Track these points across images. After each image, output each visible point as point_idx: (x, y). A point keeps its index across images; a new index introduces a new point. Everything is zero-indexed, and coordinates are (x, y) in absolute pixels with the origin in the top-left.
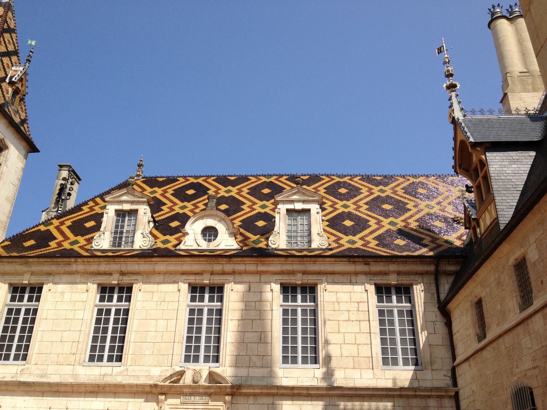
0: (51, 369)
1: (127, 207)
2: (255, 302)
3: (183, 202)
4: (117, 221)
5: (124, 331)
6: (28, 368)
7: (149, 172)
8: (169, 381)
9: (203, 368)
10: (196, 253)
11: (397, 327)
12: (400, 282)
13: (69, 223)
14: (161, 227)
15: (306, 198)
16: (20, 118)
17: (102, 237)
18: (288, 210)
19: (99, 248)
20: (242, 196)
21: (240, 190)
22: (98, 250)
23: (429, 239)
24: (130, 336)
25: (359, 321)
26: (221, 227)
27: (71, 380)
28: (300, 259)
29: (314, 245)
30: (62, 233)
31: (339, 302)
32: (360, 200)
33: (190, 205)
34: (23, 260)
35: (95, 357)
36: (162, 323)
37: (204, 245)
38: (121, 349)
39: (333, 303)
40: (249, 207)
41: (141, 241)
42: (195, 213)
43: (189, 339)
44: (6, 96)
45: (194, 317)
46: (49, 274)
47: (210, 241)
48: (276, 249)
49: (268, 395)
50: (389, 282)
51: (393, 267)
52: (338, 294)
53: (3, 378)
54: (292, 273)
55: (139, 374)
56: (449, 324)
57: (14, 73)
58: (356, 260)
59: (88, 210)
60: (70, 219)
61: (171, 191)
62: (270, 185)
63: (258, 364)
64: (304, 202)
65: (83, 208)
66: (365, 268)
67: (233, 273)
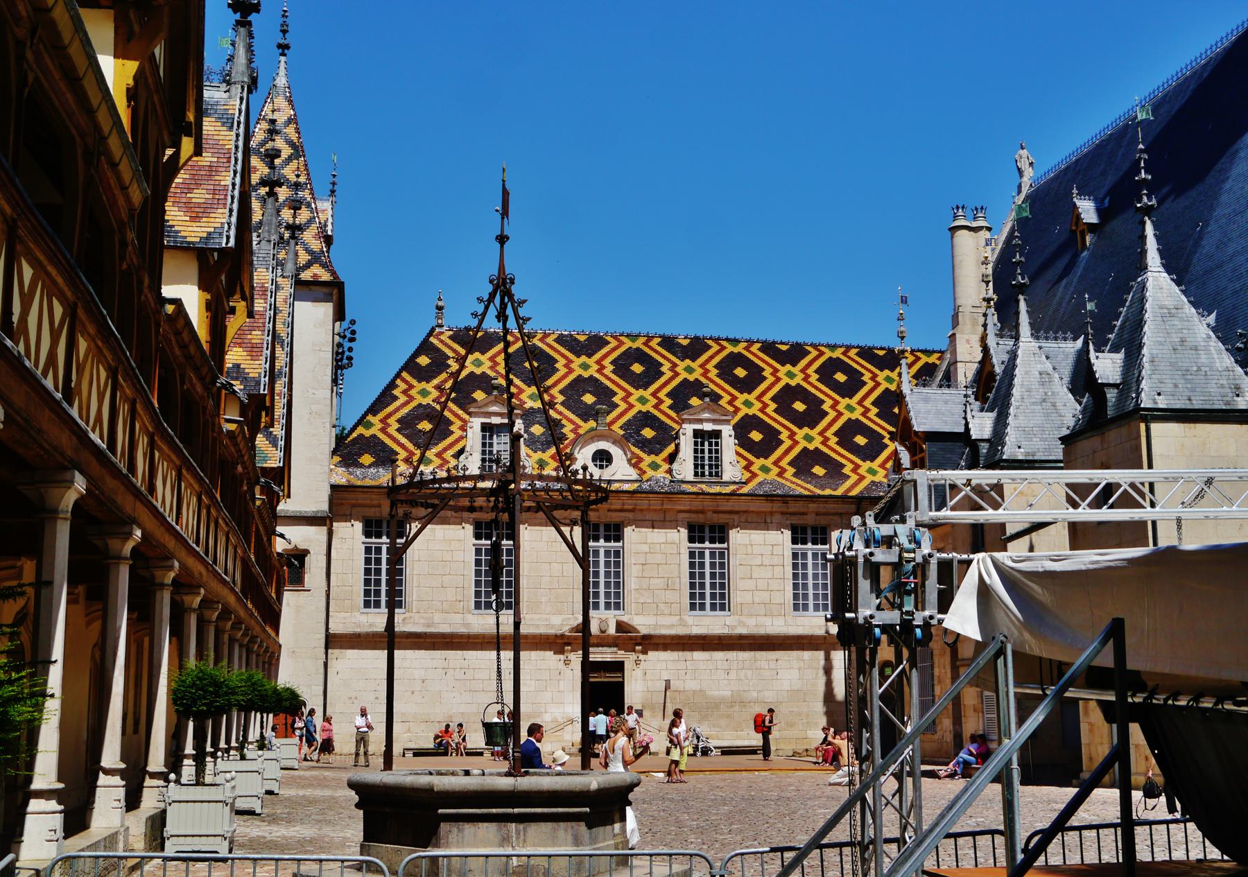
0: (437, 618)
4: (484, 437)
13: (394, 426)
15: (717, 417)
26: (615, 451)
27: (463, 630)
29: (726, 478)
48: (683, 482)
51: (812, 506)
63: (666, 612)
64: (714, 421)
65: (396, 392)
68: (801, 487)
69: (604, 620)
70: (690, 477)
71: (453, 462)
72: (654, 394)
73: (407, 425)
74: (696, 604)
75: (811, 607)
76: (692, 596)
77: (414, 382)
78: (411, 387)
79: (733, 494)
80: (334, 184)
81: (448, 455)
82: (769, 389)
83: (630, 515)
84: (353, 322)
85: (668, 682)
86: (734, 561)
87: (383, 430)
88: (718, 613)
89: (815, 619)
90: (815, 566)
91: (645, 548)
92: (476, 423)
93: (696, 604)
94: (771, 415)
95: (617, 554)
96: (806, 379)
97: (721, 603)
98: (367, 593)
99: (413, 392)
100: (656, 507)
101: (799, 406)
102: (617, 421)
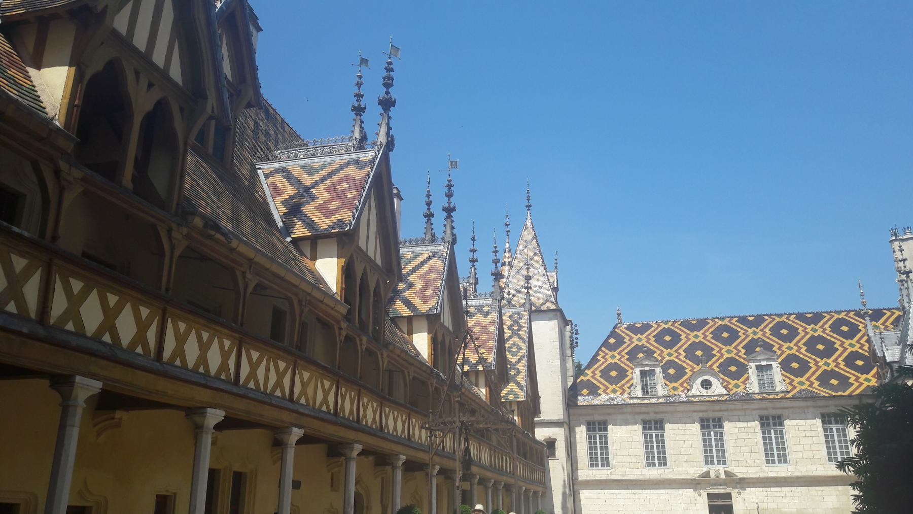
0: (628, 471)
1: (647, 368)
11: (836, 439)
26: (712, 379)
29: (778, 390)
32: (798, 342)
35: (650, 463)
38: (665, 458)
43: (705, 451)
46: (609, 414)
51: (831, 402)
54: (766, 409)
62: (726, 328)
64: (766, 360)
65: (599, 357)
67: (727, 410)
68: (825, 392)
69: (718, 471)
71: (628, 391)
72: (735, 348)
73: (605, 374)
74: (769, 460)
76: (767, 455)
77: (607, 352)
78: (606, 354)
79: (782, 398)
81: (625, 387)
82: (802, 339)
83: (726, 413)
84: (576, 325)
87: (593, 377)
90: (839, 436)
92: (637, 371)
94: (804, 353)
96: (824, 331)
97: (783, 459)
98: (591, 459)
99: (607, 357)
100: (739, 406)
101: (820, 347)
102: (715, 364)
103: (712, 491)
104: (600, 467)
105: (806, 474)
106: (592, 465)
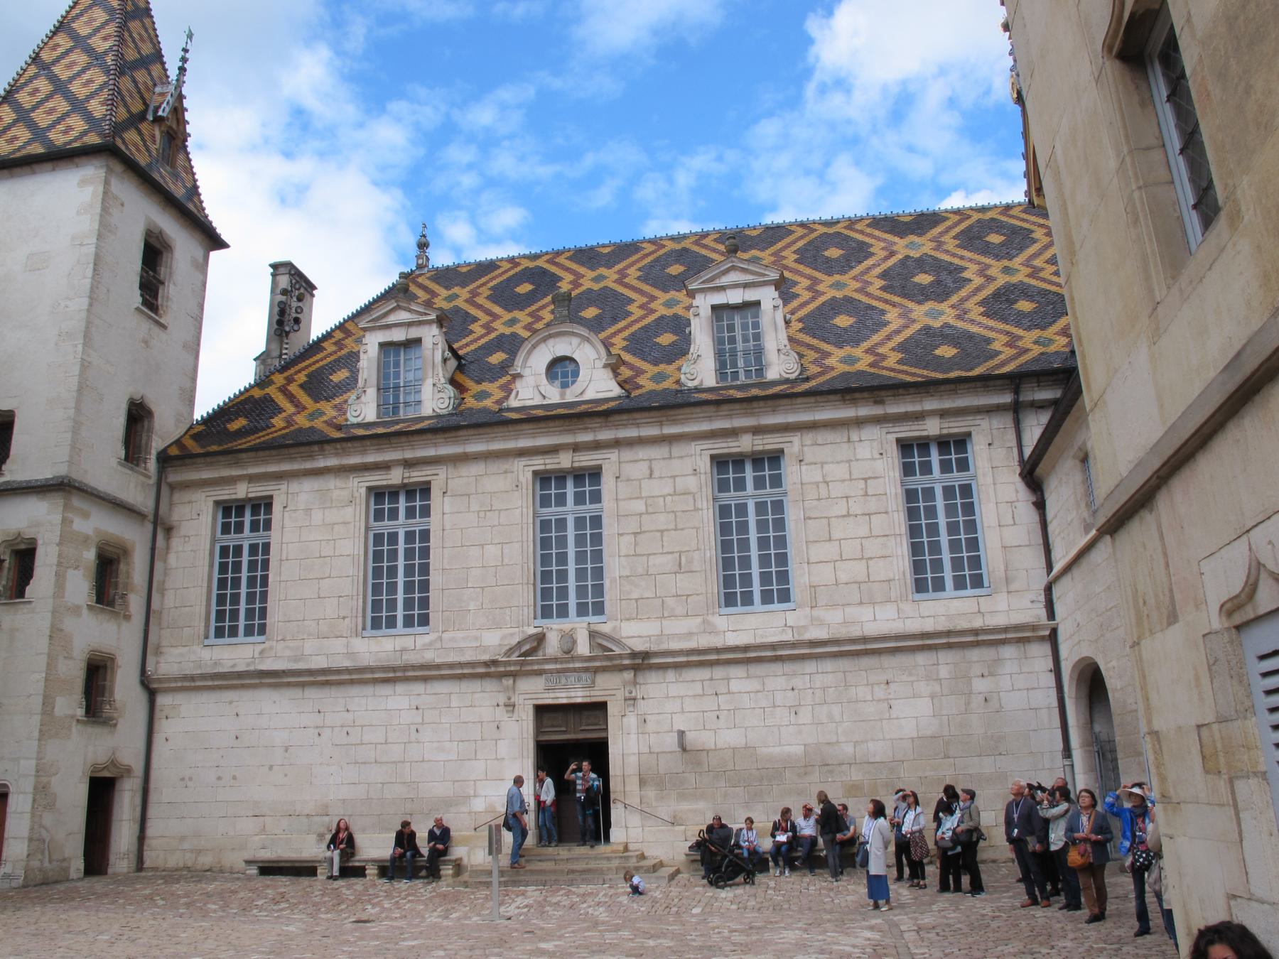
0: (309, 647)
1: (398, 335)
2: (664, 497)
3: (510, 311)
5: (425, 569)
6: (271, 648)
7: (440, 258)
8: (517, 654)
9: (577, 625)
10: (540, 413)
11: (942, 520)
12: (945, 431)
13: (302, 378)
14: (463, 369)
16: (185, 187)
17: (363, 399)
18: (714, 308)
19: (359, 420)
20: (626, 286)
21: (623, 274)
22: (359, 425)
23: (1005, 339)
24: (435, 579)
25: (869, 514)
27: (346, 663)
28: (745, 405)
29: (772, 374)
30: (291, 397)
31: (827, 483)
33: (523, 316)
34: (229, 457)
36: (492, 550)
37: (554, 395)
38: (425, 603)
39: (817, 484)
40: (641, 307)
41: (433, 398)
42: (535, 332)
43: (546, 577)
44: (153, 148)
45: (548, 537)
46: (279, 476)
47: (565, 386)
48: (698, 390)
49: (701, 664)
50: (925, 433)
51: (930, 404)
52: (826, 466)
53: (234, 666)
55: (462, 645)
56: (1040, 505)
57: (160, 99)
58: (857, 395)
59: (334, 348)
60: (303, 369)
61: (485, 292)
63: (680, 610)
65: (325, 345)
66: (877, 411)
67: (617, 444)
70: (710, 380)
74: (734, 593)
75: (949, 583)
80: (184, 60)
83: (613, 455)
85: (681, 734)
86: (792, 515)
88: (776, 606)
89: (956, 603)
91: (639, 506)
92: (372, 342)
93: (734, 593)
95: (597, 521)
97: (778, 590)
98: (220, 615)
103: (549, 698)
104: (241, 638)
105: (843, 633)
106: (219, 633)
